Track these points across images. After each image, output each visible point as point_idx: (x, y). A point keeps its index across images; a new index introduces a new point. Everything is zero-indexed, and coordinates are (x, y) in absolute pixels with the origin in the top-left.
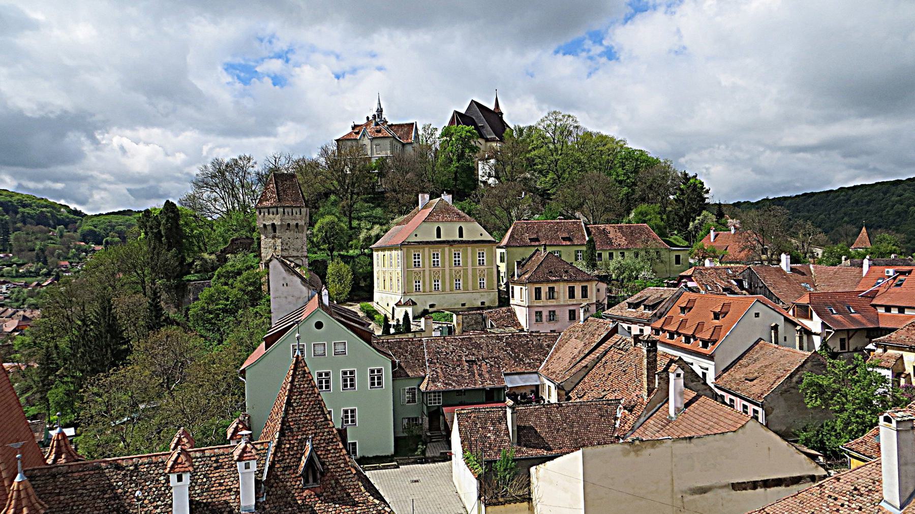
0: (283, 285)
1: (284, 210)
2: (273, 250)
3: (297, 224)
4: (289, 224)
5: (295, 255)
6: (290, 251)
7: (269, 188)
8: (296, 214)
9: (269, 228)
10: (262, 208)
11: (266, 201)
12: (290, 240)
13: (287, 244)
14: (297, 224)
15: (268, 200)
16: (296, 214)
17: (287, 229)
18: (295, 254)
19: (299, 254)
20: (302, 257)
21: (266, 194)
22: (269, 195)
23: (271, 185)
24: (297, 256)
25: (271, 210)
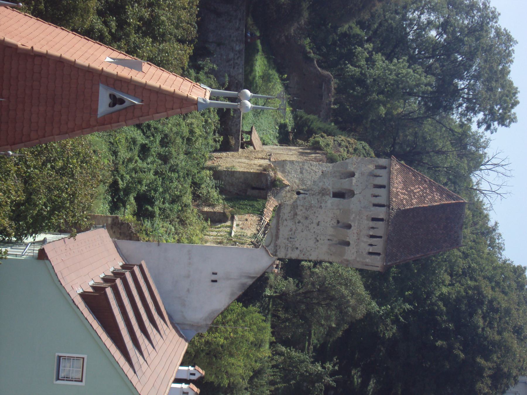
0: (215, 274)
1: (382, 220)
2: (295, 187)
3: (348, 244)
4: (349, 227)
5: (281, 233)
6: (290, 224)
7: (431, 189)
8: (371, 245)
9: (344, 184)
10: (390, 173)
11: (404, 182)
12: (314, 225)
13: (306, 218)
14: (348, 244)
15: (405, 187)
16: (371, 245)
17: (338, 222)
18: (284, 232)
19: (282, 241)
20: (276, 246)
21: (420, 183)
22: (417, 190)
23: (437, 197)
24: (277, 237)
25: (382, 192)
